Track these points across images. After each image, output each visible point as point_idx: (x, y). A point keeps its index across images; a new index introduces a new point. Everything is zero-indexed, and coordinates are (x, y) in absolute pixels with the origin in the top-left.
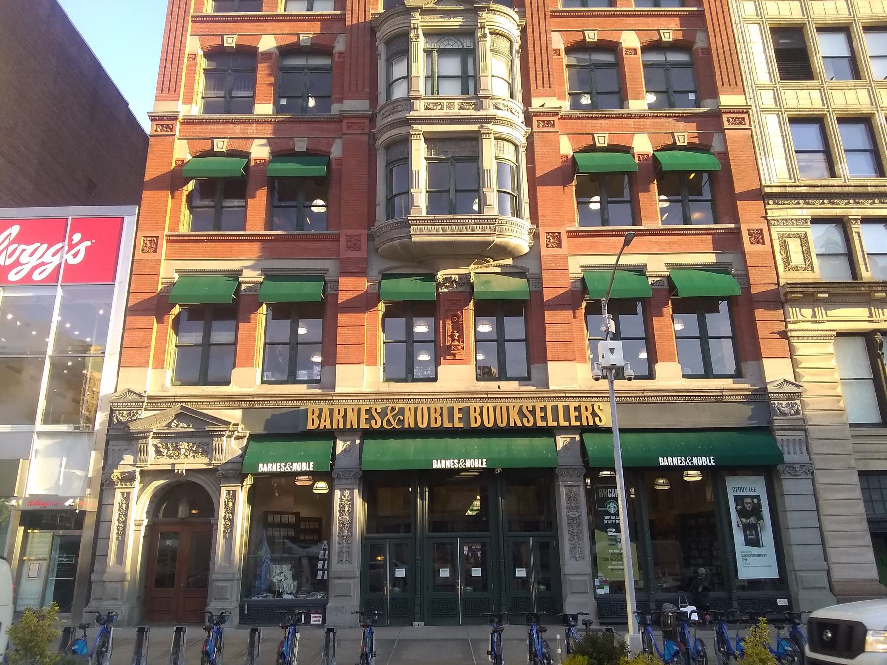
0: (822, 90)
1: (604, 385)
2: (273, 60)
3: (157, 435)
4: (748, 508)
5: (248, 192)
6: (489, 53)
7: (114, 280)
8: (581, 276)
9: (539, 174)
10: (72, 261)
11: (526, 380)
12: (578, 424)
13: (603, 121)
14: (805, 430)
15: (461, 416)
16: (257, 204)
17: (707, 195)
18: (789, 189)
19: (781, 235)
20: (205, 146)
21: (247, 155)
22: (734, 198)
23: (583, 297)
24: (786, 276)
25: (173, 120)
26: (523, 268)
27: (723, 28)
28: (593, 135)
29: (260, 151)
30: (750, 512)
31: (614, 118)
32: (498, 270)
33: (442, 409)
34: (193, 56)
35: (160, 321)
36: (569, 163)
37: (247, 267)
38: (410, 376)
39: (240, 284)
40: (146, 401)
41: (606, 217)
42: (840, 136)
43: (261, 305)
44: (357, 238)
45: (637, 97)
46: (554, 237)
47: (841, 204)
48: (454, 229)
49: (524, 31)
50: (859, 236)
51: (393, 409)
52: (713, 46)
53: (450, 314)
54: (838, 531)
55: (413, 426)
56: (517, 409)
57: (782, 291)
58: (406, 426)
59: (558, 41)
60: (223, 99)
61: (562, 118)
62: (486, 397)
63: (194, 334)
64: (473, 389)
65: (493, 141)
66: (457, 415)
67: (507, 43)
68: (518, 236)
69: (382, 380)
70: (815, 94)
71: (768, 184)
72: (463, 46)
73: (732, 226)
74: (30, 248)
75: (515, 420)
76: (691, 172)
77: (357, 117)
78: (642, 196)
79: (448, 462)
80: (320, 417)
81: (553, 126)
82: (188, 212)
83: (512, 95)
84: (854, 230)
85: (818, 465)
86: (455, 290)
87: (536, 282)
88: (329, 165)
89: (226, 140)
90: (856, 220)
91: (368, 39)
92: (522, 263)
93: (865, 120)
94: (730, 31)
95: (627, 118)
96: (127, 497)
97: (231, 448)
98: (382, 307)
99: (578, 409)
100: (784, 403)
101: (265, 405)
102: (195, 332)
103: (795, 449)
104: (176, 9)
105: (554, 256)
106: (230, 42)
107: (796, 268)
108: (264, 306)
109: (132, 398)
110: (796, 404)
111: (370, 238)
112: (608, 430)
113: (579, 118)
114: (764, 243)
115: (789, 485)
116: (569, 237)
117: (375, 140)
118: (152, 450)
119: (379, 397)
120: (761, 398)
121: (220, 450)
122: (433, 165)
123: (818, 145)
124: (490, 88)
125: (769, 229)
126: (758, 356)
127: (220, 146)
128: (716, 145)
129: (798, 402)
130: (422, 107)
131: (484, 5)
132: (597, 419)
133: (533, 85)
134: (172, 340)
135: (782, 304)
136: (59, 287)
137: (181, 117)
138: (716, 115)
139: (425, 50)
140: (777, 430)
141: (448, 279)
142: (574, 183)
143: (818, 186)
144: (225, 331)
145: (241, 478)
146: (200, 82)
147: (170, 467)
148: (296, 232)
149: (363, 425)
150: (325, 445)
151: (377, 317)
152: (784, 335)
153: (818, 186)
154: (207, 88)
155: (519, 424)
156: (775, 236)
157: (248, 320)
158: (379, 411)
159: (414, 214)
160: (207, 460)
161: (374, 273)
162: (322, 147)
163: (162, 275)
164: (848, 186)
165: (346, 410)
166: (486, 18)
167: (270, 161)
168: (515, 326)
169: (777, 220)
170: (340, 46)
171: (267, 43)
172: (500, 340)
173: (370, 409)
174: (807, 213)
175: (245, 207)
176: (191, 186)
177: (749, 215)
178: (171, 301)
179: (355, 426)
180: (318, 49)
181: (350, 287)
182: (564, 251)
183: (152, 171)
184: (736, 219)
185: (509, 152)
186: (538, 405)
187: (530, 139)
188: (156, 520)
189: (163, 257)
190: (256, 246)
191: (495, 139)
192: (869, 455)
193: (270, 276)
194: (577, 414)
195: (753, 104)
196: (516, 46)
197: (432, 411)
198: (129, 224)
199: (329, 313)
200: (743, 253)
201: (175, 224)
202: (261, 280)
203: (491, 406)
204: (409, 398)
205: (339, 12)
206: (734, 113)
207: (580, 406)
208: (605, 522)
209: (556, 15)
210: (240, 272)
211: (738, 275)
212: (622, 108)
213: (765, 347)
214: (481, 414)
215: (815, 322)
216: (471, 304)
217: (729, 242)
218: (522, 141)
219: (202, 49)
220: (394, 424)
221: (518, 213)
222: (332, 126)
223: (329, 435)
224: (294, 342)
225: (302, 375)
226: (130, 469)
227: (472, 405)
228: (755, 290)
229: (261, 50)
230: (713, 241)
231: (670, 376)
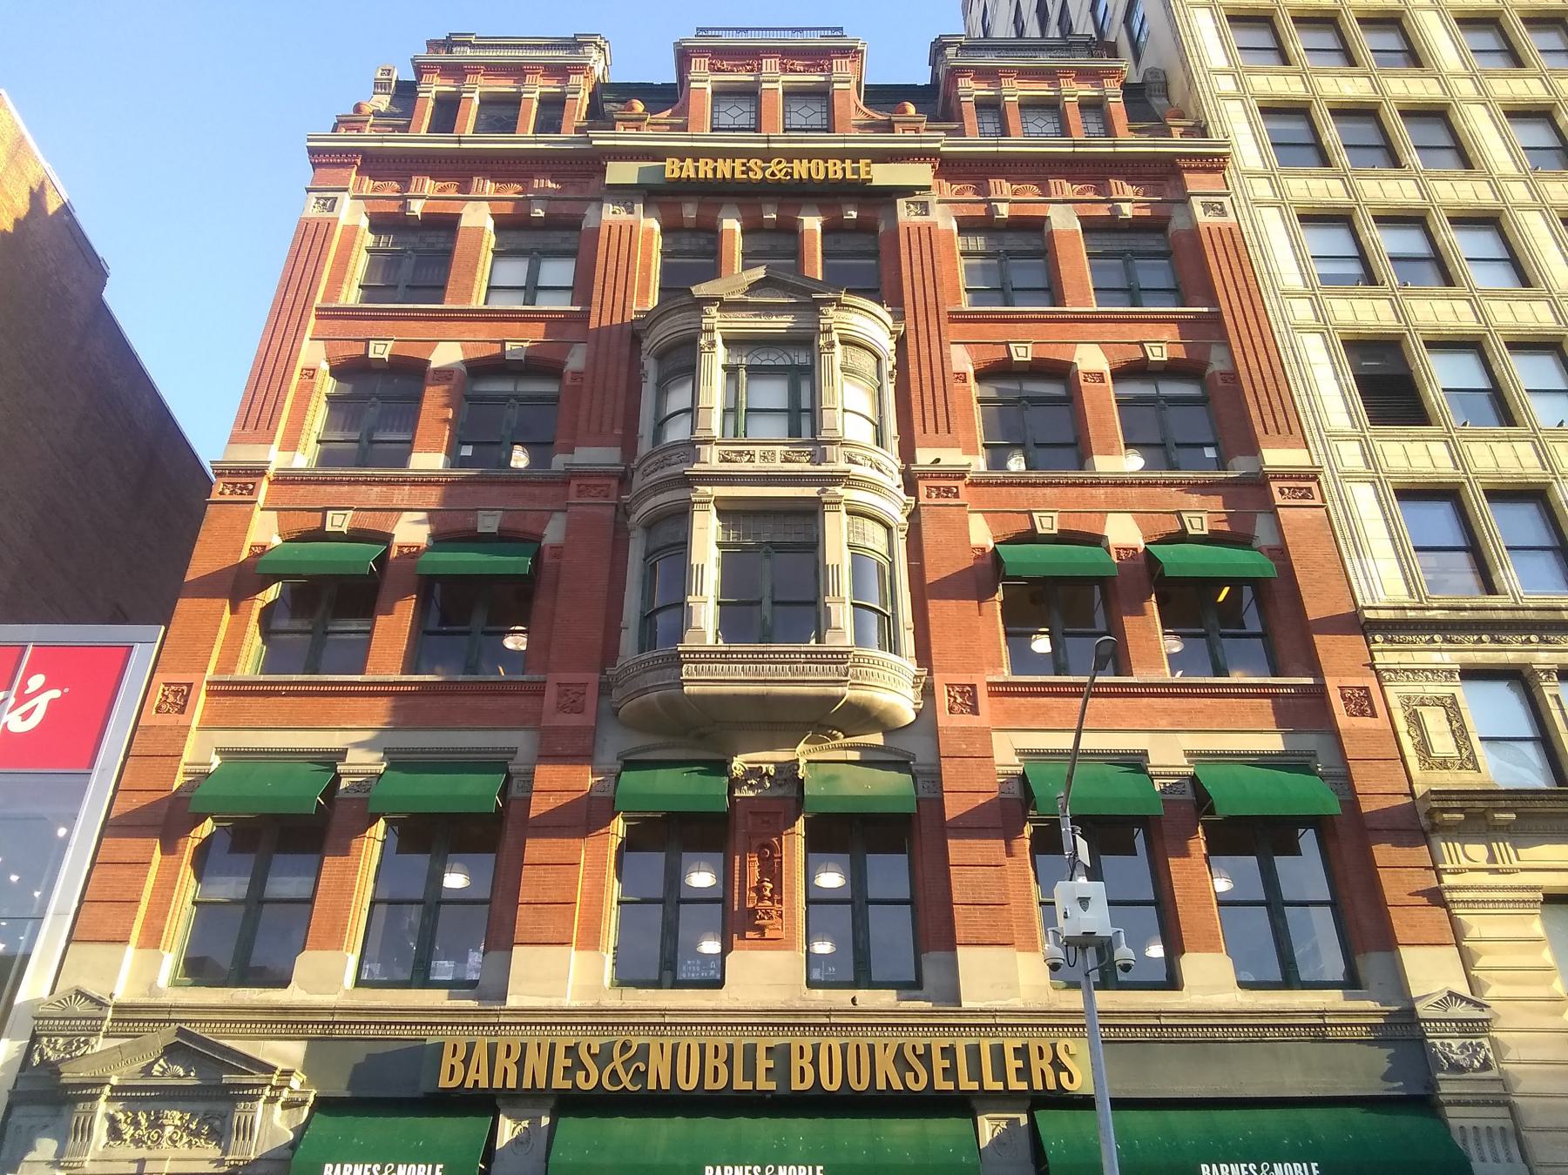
0: (1448, 441)
1: (1073, 1000)
2: (454, 381)
5: (380, 604)
6: (838, 374)
7: (91, 765)
8: (1019, 770)
9: (931, 577)
11: (911, 986)
12: (1024, 1086)
13: (1048, 491)
15: (771, 1064)
16: (393, 629)
17: (1253, 623)
18: (1411, 614)
19: (1407, 701)
20: (310, 522)
21: (386, 539)
22: (1305, 630)
23: (1025, 813)
24: (1425, 780)
25: (256, 475)
26: (902, 753)
27: (1257, 340)
28: (1030, 513)
29: (411, 532)
31: (1067, 485)
32: (855, 755)
33: (730, 1048)
34: (310, 373)
35: (169, 848)
36: (988, 561)
37: (358, 745)
38: (668, 975)
39: (337, 778)
41: (1062, 660)
42: (1495, 524)
43: (373, 820)
44: (580, 689)
45: (1108, 451)
46: (962, 694)
47: (1516, 641)
48: (767, 671)
49: (901, 342)
50: (1559, 703)
51: (625, 1047)
52: (1242, 369)
55: (666, 1085)
56: (891, 1052)
57: (1422, 809)
58: (652, 1085)
59: (962, 360)
60: (355, 446)
61: (972, 484)
62: (824, 1023)
63: (234, 880)
64: (798, 1005)
65: (845, 518)
66: (763, 1063)
67: (872, 361)
68: (892, 687)
69: (607, 981)
70: (1439, 450)
71: (1369, 603)
72: (793, 362)
73: (1310, 681)
75: (888, 1076)
76: (1219, 582)
77: (598, 475)
78: (1128, 621)
80: (466, 1062)
81: (956, 496)
82: (258, 640)
83: (880, 441)
84: (1547, 692)
86: (769, 794)
87: (930, 780)
88: (537, 558)
90: (1548, 672)
91: (626, 351)
92: (901, 743)
93: (1534, 495)
94: (1270, 344)
95: (1091, 485)
98: (619, 827)
99: (1022, 1052)
101: (356, 1031)
102: (238, 874)
104: (290, 296)
105: (963, 729)
106: (380, 351)
107: (1444, 764)
108: (382, 823)
111: (605, 689)
112: (1086, 1103)
113: (1003, 485)
114: (1374, 715)
116: (991, 694)
117: (627, 515)
119: (596, 1019)
122: (731, 556)
123: (1454, 537)
124: (839, 428)
125: (1382, 688)
126: (1388, 943)
127: (338, 522)
128: (1262, 531)
130: (716, 457)
131: (831, 295)
133: (918, 428)
134: (187, 888)
135: (1425, 834)
137: (271, 472)
138: (1259, 483)
139: (725, 367)
141: (751, 773)
142: (999, 596)
143: (1465, 609)
144: (297, 872)
146: (317, 417)
148: (460, 678)
149: (559, 1083)
151: (605, 846)
152: (1436, 897)
153: (1465, 609)
154: (330, 425)
155: (897, 1085)
156: (1394, 702)
157: (345, 851)
158: (595, 1050)
159: (689, 642)
161: (608, 756)
162: (528, 525)
163: (186, 758)
164: (1524, 609)
165: (524, 1046)
166: (832, 317)
167: (428, 549)
168: (889, 874)
169: (1395, 671)
170: (576, 361)
171: (446, 355)
172: (857, 900)
173: (577, 1044)
174: (1450, 658)
175: (370, 632)
176: (272, 593)
178: (194, 808)
179: (541, 1084)
180: (535, 366)
181: (558, 784)
182: (982, 720)
183: (201, 564)
184: (1315, 668)
185: (875, 538)
186: (938, 1043)
187: (914, 516)
189: (195, 723)
190: (383, 704)
191: (848, 513)
193: (399, 761)
194: (1020, 1064)
195: (1325, 463)
196: (888, 366)
197: (710, 1052)
198: (142, 658)
199: (509, 839)
200: (1336, 734)
201: (231, 657)
202: (381, 769)
203: (836, 1043)
204: (661, 1023)
205: (578, 308)
206: (1291, 479)
207: (1026, 1047)
209: (958, 318)
210: (342, 754)
212: (1081, 467)
213: (1398, 918)
214: (815, 1062)
215: (1496, 871)
216: (800, 825)
217: (1306, 711)
218: (899, 519)
219: (328, 360)
220: (626, 1080)
221: (894, 648)
222: (550, 491)
223: (483, 1104)
224: (435, 900)
225: (443, 969)
227: (795, 1042)
228: (1367, 806)
229: (433, 366)
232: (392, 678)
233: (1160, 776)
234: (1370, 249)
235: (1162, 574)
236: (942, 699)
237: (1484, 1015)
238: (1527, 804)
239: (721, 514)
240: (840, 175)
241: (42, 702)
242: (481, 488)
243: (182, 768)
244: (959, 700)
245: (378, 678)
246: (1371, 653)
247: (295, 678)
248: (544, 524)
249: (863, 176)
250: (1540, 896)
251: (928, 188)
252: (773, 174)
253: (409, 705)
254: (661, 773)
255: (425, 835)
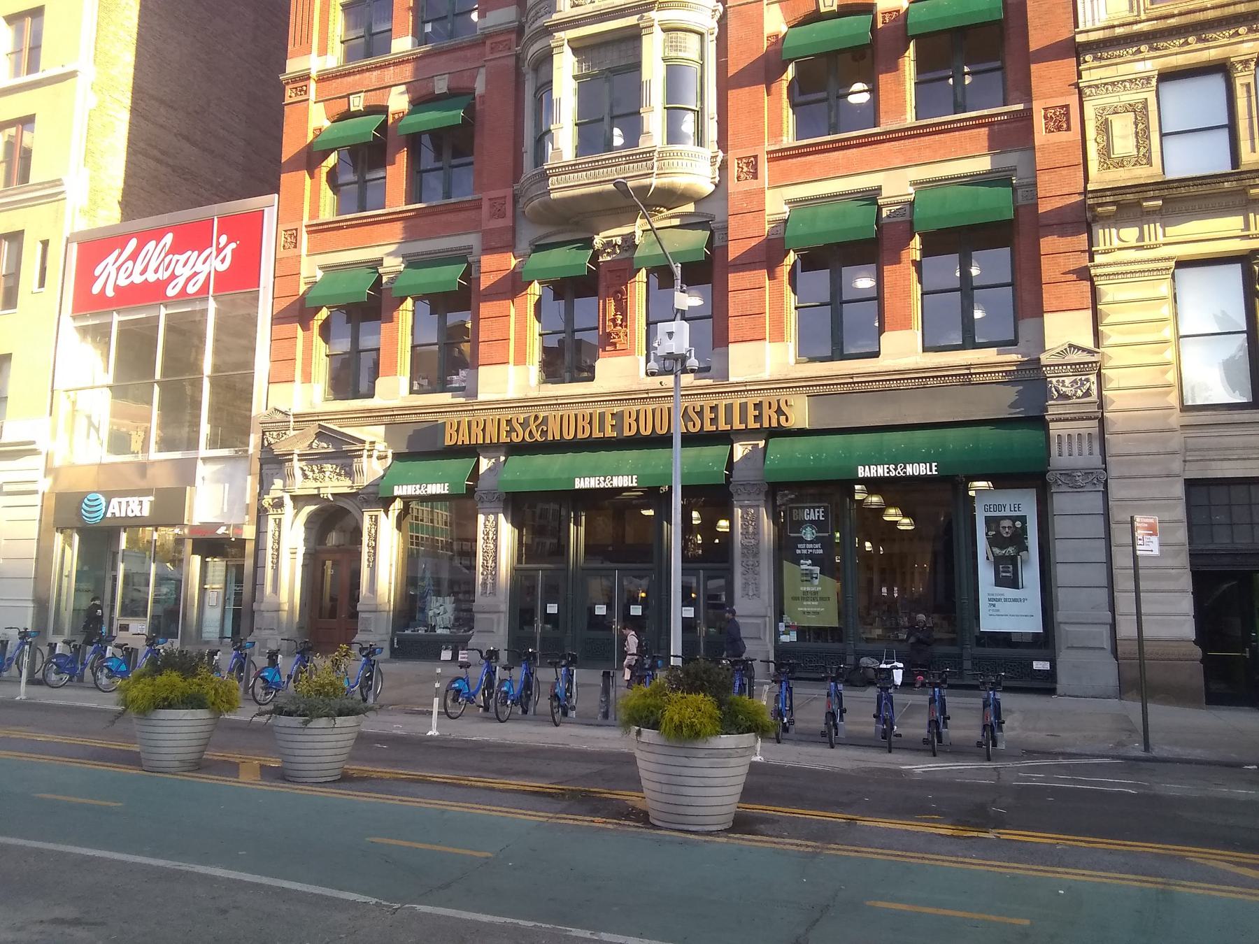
3: (302, 457)
4: (1006, 533)
10: (222, 267)
11: (702, 371)
14: (1102, 421)
16: (397, 173)
18: (1119, 31)
20: (340, 107)
21: (383, 110)
24: (1100, 177)
29: (398, 102)
30: (1009, 540)
32: (676, 222)
35: (306, 327)
37: (389, 254)
39: (380, 277)
40: (292, 419)
43: (403, 299)
46: (748, 164)
47: (1222, 37)
53: (612, 290)
54: (1157, 568)
66: (609, 421)
68: (693, 170)
73: (1020, 107)
74: (183, 258)
77: (501, 33)
79: (592, 480)
80: (457, 431)
82: (330, 193)
85: (1114, 471)
89: (362, 95)
92: (707, 208)
96: (279, 524)
97: (371, 469)
100: (1068, 381)
103: (1080, 449)
108: (409, 301)
109: (279, 417)
110: (1088, 380)
114: (1068, 129)
115: (1061, 502)
118: (298, 473)
120: (1033, 375)
121: (361, 472)
127: (357, 103)
129: (1093, 378)
132: (782, 418)
136: (211, 299)
137: (314, 75)
140: (1053, 421)
141: (609, 244)
143: (1173, 16)
145: (386, 502)
147: (316, 492)
149: (504, 438)
150: (466, 464)
152: (1084, 274)
153: (1173, 16)
160: (349, 483)
167: (410, 113)
169: (1097, 86)
177: (1049, 82)
181: (495, 267)
183: (289, 150)
184: (1027, 96)
187: (722, 22)
188: (318, 548)
190: (399, 226)
191: (664, 30)
192: (1212, 455)
193: (413, 262)
197: (580, 418)
201: (315, 212)
204: (555, 403)
208: (798, 552)
210: (379, 262)
211: (1022, 186)
213: (1049, 296)
214: (637, 420)
217: (1013, 134)
222: (476, 51)
223: (471, 451)
226: (279, 494)
230: (991, 138)
231: (902, 350)
232: (398, 209)
236: (733, 170)
237: (1093, 359)
238: (1174, 191)
239: (575, 51)
241: (228, 251)
242: (434, 59)
243: (302, 281)
244: (745, 169)
245: (391, 210)
247: (348, 216)
248: (474, 79)
250: (1173, 264)
253: (415, 225)
254: (555, 252)
255: (439, 303)
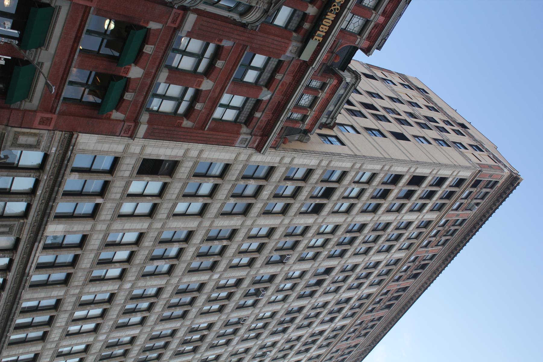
233: (37, 52)
234: (206, 179)
235: (113, 80)
240: (321, 29)
246: (62, 131)
249: (315, 37)
251: (299, 56)
252: (335, 5)
